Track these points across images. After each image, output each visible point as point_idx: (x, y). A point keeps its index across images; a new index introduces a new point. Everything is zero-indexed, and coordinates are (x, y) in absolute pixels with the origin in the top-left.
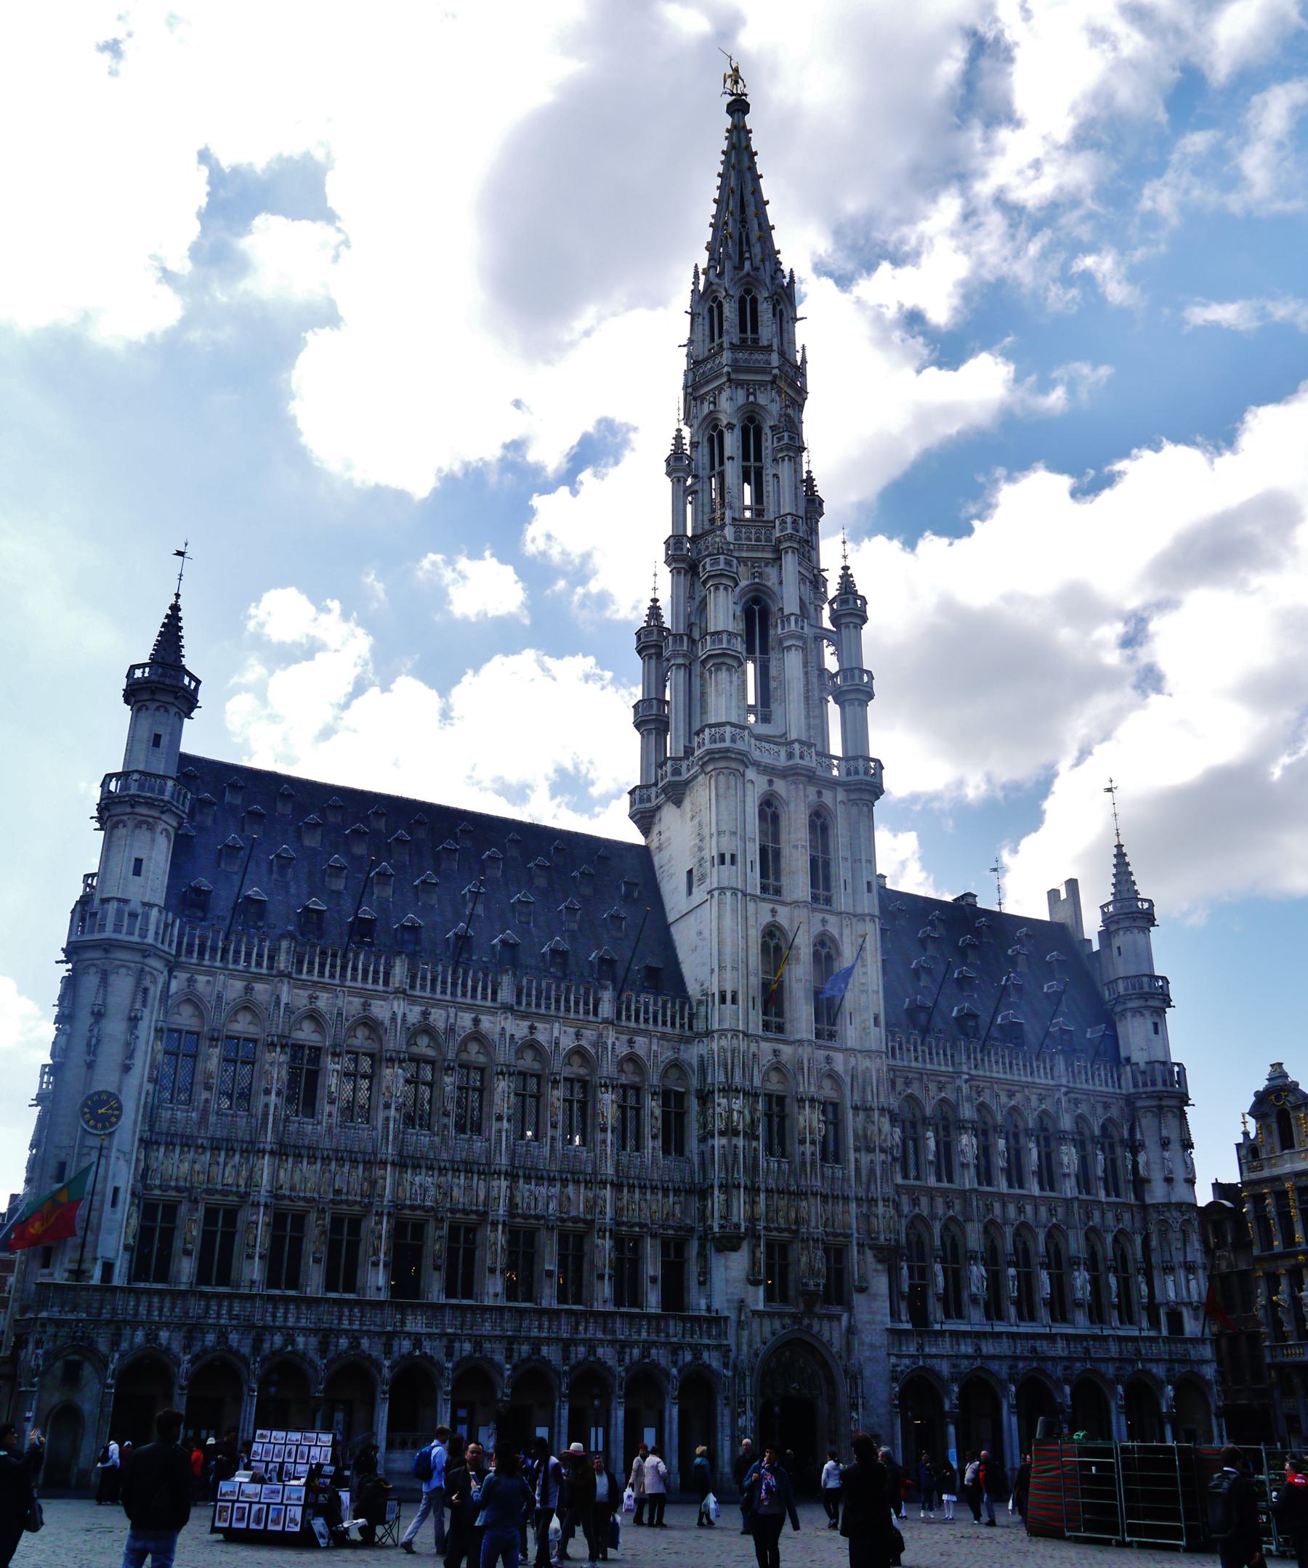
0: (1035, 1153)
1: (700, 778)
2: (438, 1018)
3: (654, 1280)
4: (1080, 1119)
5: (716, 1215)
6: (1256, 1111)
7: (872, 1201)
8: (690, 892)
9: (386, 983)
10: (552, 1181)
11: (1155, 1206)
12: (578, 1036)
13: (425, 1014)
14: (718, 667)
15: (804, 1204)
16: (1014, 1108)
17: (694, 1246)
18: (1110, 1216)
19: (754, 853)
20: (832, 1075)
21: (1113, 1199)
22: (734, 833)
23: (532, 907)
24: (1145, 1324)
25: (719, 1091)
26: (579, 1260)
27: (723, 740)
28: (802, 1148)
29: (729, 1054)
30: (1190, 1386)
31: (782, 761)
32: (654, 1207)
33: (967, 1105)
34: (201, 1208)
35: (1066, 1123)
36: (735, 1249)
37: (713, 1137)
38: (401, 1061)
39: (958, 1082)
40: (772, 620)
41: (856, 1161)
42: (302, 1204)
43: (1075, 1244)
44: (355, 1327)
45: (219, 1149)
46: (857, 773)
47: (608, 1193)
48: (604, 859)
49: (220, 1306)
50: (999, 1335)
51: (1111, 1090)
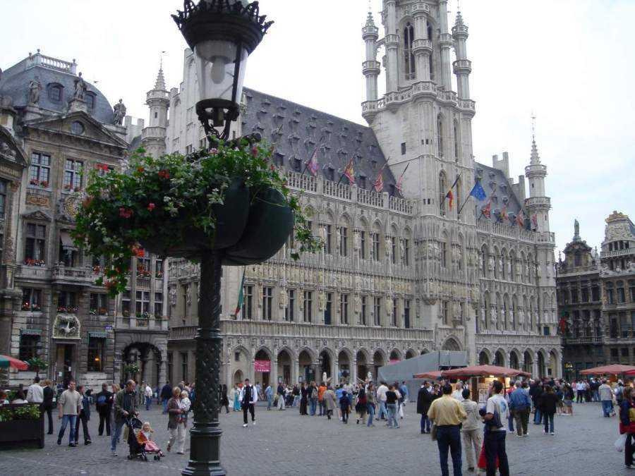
0: (510, 265)
2: (332, 206)
3: (403, 316)
5: (428, 291)
6: (567, 252)
8: (404, 152)
9: (315, 191)
10: (371, 276)
11: (543, 288)
12: (376, 215)
13: (328, 205)
14: (423, 55)
16: (504, 249)
17: (413, 304)
18: (528, 290)
19: (436, 141)
20: (460, 236)
24: (537, 330)
26: (379, 307)
30: (553, 353)
31: (444, 100)
32: (403, 287)
36: (433, 304)
37: (425, 259)
40: (433, 33)
41: (468, 269)
43: (521, 303)
44: (325, 337)
46: (468, 106)
47: (389, 281)
50: (505, 336)
51: (531, 242)
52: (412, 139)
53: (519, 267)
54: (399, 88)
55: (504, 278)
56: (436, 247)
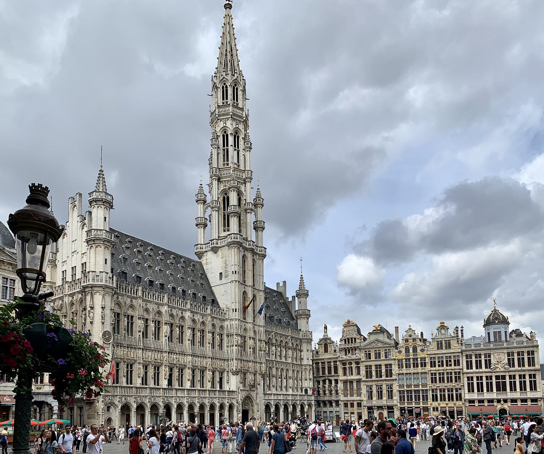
0: (285, 351)
1: (226, 247)
2: (174, 312)
4: (292, 343)
7: (261, 363)
12: (203, 318)
13: (171, 310)
15: (250, 364)
16: (281, 341)
21: (296, 363)
22: (238, 266)
23: (184, 279)
24: (300, 392)
25: (235, 335)
27: (237, 239)
28: (250, 350)
29: (238, 325)
32: (218, 364)
33: (274, 339)
34: (126, 363)
35: (290, 345)
36: (238, 375)
38: (169, 324)
39: (272, 334)
42: (148, 363)
45: (129, 347)
48: (194, 265)
49: (140, 390)
52: (227, 270)
53: (290, 352)
54: (219, 237)
55: (281, 358)
56: (239, 339)
